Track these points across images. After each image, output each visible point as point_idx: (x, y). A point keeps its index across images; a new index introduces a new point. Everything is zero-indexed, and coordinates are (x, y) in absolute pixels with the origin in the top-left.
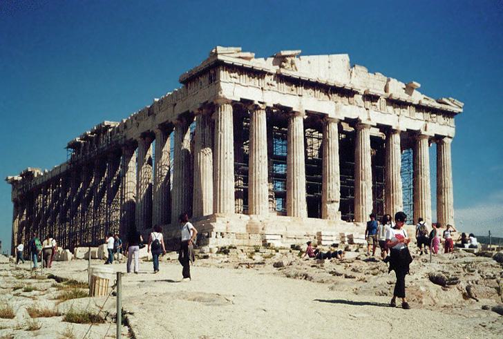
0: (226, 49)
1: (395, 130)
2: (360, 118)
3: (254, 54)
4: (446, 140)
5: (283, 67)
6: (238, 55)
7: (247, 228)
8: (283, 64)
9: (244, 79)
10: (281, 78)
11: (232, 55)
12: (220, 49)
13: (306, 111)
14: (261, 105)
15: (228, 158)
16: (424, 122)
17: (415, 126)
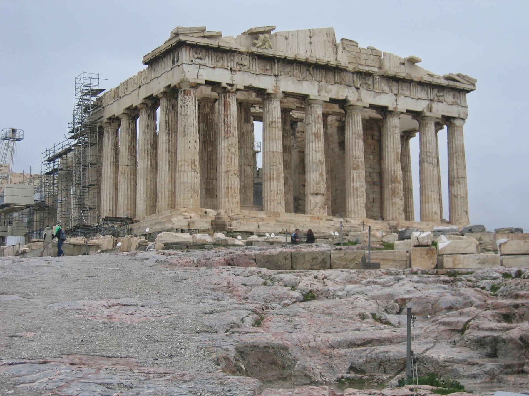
2: (349, 99)
5: (255, 45)
7: (212, 225)
13: (283, 92)
14: (229, 88)
16: (427, 102)
17: (420, 106)
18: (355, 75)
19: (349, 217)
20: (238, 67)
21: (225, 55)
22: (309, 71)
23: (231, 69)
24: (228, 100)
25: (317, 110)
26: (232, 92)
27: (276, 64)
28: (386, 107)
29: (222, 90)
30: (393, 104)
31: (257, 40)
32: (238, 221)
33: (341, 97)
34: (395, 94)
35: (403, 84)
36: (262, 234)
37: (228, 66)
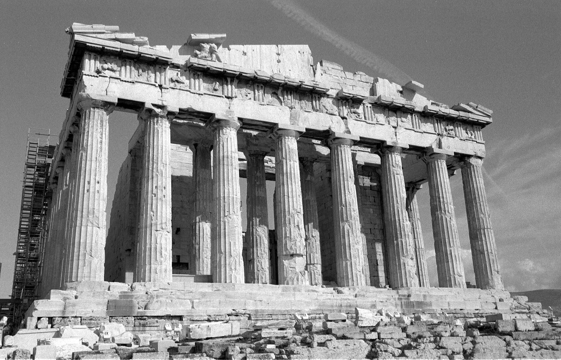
0: (89, 26)
1: (391, 147)
2: (333, 130)
3: (146, 39)
4: (473, 161)
5: (196, 56)
6: (113, 36)
8: (198, 52)
9: (128, 72)
10: (194, 71)
11: (99, 36)
12: (77, 27)
13: (240, 119)
14: (158, 111)
15: (91, 190)
16: (436, 137)
18: (340, 103)
19: (341, 287)
20: (172, 85)
21: (152, 68)
22: (277, 94)
23: (160, 86)
24: (156, 126)
25: (289, 143)
26: (162, 117)
27: (229, 83)
28: (383, 142)
29: (148, 113)
30: (392, 138)
31: (200, 51)
32: (161, 299)
33: (321, 127)
34: (393, 127)
35: (402, 114)
36: (195, 318)
37: (156, 82)
